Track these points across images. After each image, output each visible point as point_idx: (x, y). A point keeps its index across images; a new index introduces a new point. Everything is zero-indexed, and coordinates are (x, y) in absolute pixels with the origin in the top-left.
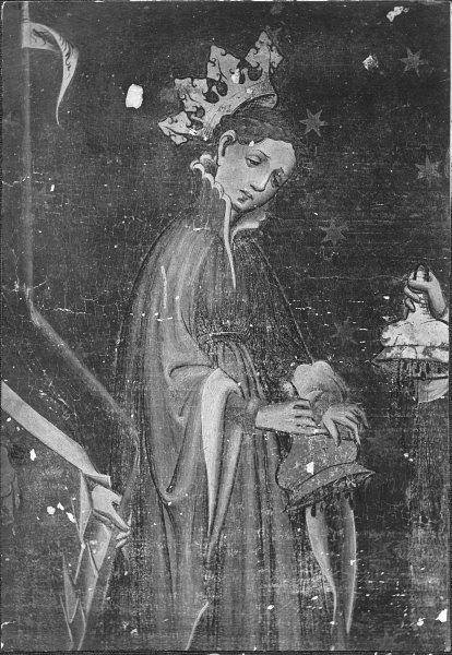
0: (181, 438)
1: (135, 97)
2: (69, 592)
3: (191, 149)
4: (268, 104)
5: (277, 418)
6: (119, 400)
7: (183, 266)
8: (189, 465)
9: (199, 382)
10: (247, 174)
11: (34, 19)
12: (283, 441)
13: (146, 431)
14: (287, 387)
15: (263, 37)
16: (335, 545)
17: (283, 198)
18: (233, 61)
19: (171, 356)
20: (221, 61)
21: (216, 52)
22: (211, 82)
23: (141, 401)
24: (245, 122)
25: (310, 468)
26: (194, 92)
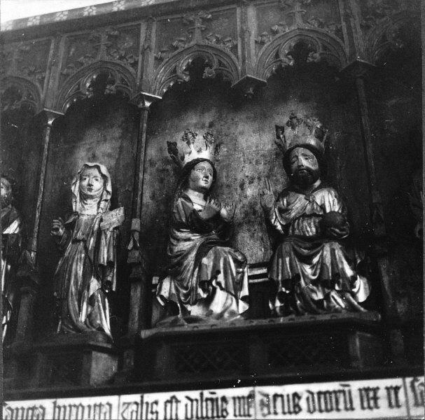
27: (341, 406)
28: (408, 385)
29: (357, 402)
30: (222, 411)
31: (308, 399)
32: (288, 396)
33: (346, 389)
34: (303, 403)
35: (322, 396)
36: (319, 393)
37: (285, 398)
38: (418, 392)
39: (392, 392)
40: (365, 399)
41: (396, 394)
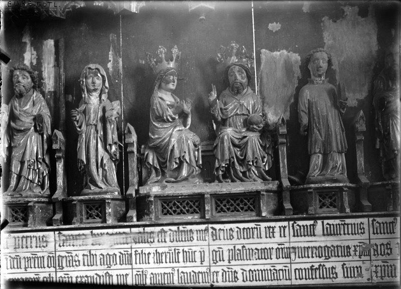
27: (255, 236)
28: (291, 225)
30: (190, 238)
32: (227, 230)
33: (258, 227)
34: (235, 234)
36: (244, 229)
37: (225, 231)
38: (295, 229)
39: (282, 229)
41: (284, 230)
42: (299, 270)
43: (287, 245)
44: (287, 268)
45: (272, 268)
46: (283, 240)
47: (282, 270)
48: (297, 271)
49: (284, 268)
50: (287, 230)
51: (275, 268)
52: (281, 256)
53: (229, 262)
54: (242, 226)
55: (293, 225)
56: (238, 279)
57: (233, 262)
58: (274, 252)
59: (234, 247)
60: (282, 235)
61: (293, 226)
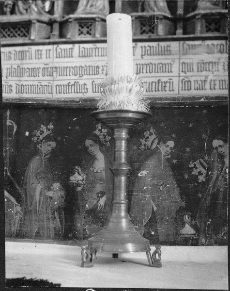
0: (32, 197)
1: (27, 134)
2: (12, 226)
3: (38, 143)
4: (51, 135)
5: (50, 194)
6: (21, 190)
7: (35, 165)
8: (34, 203)
9: (36, 186)
10: (47, 148)
11: (10, 120)
12: (51, 198)
13: (26, 196)
14: (52, 188)
15: (51, 123)
16: (60, 218)
17: (53, 152)
18: (45, 127)
19: (32, 181)
20: (43, 128)
21: (42, 126)
22: (41, 131)
23: (26, 190)
24: (48, 138)
25: (56, 203)
26: (38, 133)
28: (55, 49)
29: (33, 56)
31: (14, 54)
33: (30, 50)
34: (12, 56)
35: (20, 53)
38: (58, 52)
39: (48, 51)
40: (37, 54)
42: (59, 86)
43: (51, 65)
44: (50, 85)
45: (39, 84)
46: (48, 61)
47: (46, 86)
48: (58, 86)
49: (48, 84)
50: (51, 52)
51: (41, 84)
52: (46, 75)
53: (7, 78)
54: (18, 49)
55: (56, 48)
56: (12, 91)
57: (10, 78)
58: (41, 71)
59: (12, 66)
60: (48, 57)
61: (56, 49)
